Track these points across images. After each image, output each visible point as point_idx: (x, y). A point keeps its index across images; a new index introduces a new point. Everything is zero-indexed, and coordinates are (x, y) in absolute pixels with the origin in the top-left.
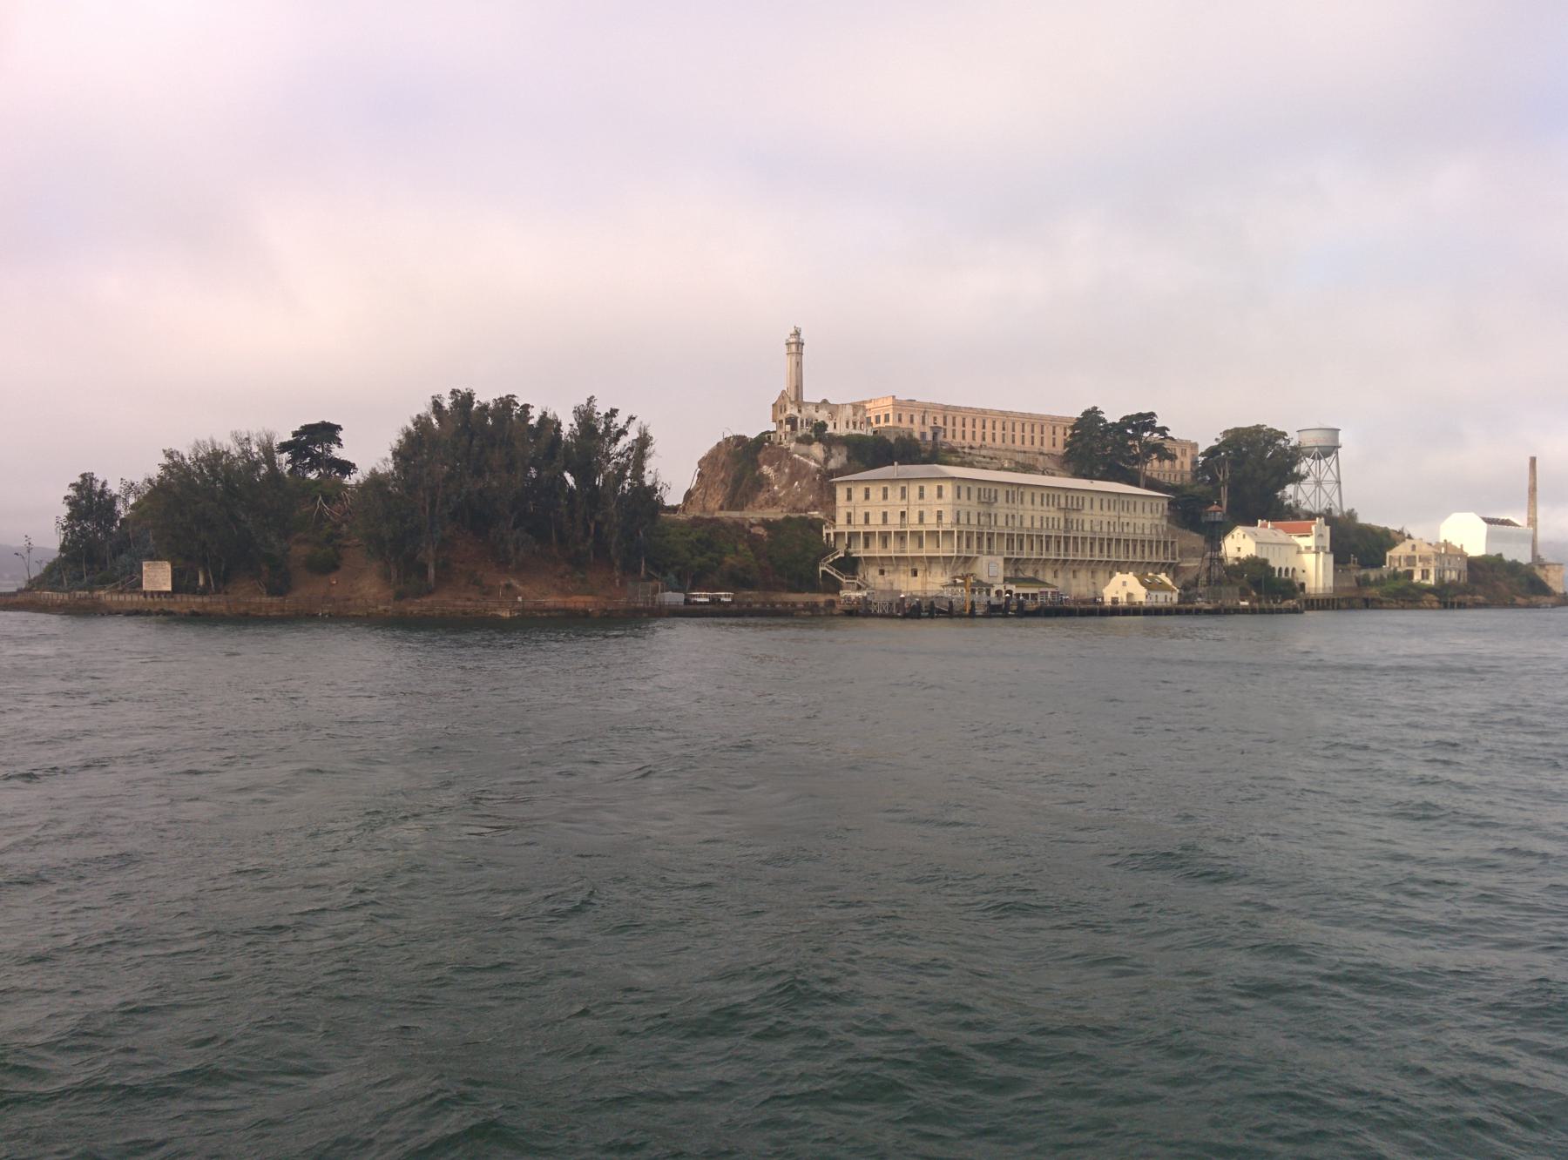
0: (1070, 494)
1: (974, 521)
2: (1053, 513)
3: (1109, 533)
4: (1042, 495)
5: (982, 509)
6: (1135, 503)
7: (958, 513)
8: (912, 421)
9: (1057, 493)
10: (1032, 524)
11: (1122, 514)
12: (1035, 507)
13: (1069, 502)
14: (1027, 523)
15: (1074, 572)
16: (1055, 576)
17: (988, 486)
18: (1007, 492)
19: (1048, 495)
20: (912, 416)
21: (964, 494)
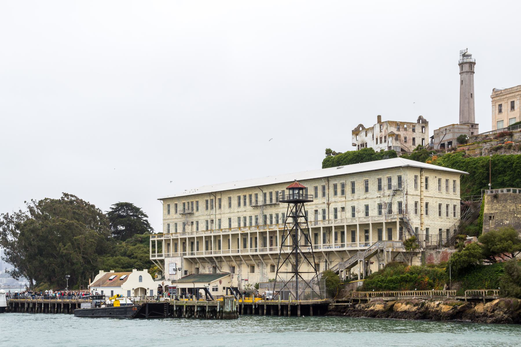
0: (267, 191)
1: (180, 230)
2: (248, 211)
3: (316, 222)
4: (239, 198)
5: (183, 219)
6: (353, 184)
7: (169, 225)
8: (513, 107)
9: (253, 193)
10: (230, 225)
11: (332, 199)
12: (232, 210)
13: (268, 198)
14: (225, 225)
15: (273, 266)
16: (253, 271)
17: (190, 200)
18: (207, 201)
19: (245, 196)
20: (513, 103)
21: (172, 210)
